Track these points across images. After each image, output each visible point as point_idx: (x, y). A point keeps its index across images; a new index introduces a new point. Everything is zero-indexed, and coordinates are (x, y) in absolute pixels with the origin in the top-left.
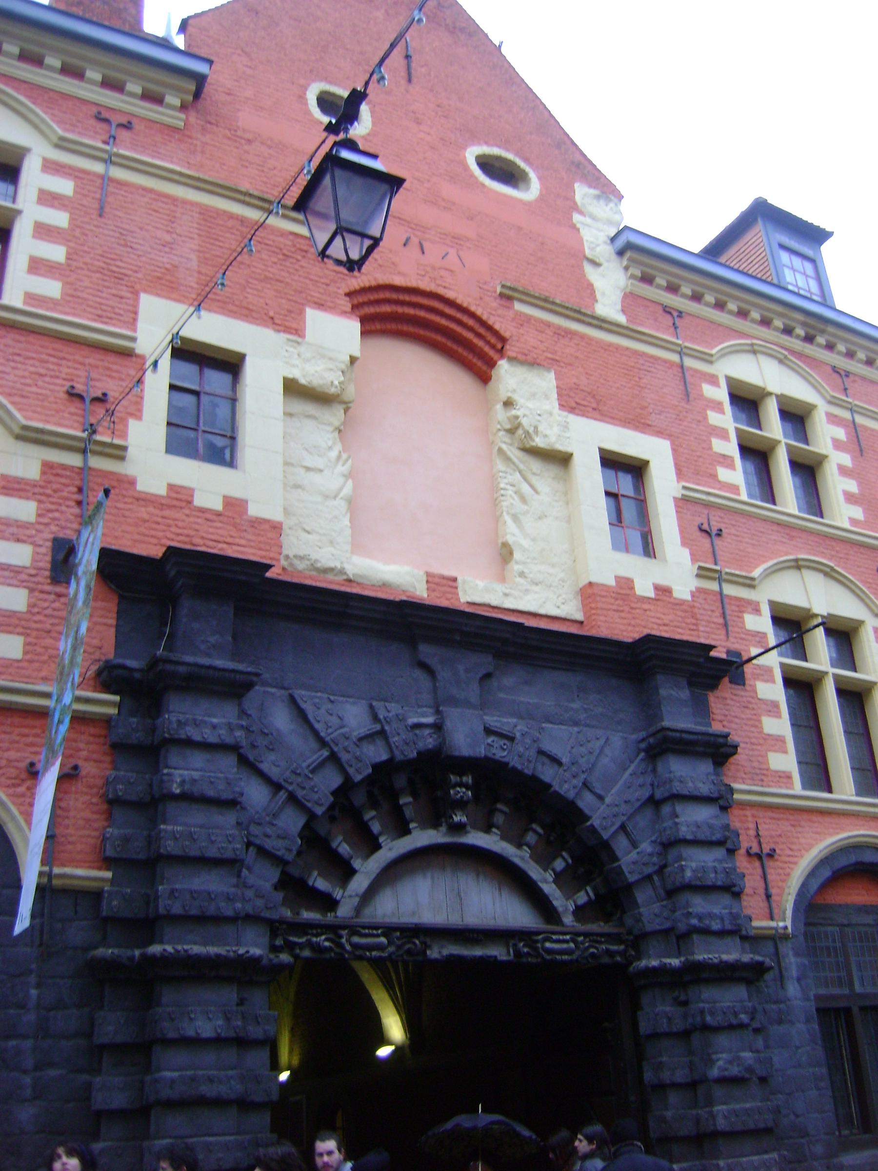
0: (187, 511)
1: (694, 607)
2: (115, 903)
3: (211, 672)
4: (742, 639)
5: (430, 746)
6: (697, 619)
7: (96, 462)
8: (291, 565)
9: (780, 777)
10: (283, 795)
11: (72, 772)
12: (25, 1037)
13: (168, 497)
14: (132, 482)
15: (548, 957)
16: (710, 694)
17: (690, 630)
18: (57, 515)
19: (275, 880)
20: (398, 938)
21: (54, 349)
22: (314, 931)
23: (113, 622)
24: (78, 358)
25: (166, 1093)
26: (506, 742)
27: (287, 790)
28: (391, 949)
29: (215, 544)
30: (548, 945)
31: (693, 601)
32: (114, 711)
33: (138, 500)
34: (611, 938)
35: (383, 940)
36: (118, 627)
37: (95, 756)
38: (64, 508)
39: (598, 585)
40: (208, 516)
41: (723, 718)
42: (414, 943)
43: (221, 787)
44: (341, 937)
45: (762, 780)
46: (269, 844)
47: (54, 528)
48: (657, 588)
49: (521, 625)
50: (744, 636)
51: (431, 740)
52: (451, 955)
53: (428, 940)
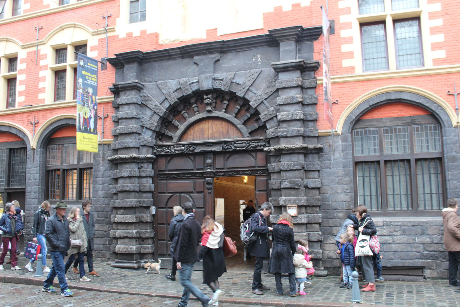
0: (131, 39)
1: (311, 7)
2: (113, 146)
4: (336, 13)
5: (196, 89)
6: (312, 12)
7: (110, 34)
8: (164, 43)
9: (348, 69)
10: (153, 112)
11: (107, 116)
12: (100, 177)
13: (127, 37)
14: (118, 36)
15: (235, 149)
16: (315, 42)
17: (308, 18)
18: (102, 52)
20: (187, 147)
21: (100, 7)
23: (115, 76)
24: (105, 7)
25: (119, 190)
26: (221, 82)
28: (185, 150)
29: (138, 46)
30: (235, 145)
31: (311, 5)
32: (113, 99)
33: (119, 41)
34: (259, 140)
35: (183, 148)
36: (116, 77)
37: (112, 111)
38: (103, 50)
39: (266, 13)
40: (137, 38)
41: (320, 51)
44: (171, 148)
45: (337, 72)
46: (148, 126)
47: (101, 56)
48: (293, 6)
49: (223, 41)
50: (336, 12)
53: (195, 147)
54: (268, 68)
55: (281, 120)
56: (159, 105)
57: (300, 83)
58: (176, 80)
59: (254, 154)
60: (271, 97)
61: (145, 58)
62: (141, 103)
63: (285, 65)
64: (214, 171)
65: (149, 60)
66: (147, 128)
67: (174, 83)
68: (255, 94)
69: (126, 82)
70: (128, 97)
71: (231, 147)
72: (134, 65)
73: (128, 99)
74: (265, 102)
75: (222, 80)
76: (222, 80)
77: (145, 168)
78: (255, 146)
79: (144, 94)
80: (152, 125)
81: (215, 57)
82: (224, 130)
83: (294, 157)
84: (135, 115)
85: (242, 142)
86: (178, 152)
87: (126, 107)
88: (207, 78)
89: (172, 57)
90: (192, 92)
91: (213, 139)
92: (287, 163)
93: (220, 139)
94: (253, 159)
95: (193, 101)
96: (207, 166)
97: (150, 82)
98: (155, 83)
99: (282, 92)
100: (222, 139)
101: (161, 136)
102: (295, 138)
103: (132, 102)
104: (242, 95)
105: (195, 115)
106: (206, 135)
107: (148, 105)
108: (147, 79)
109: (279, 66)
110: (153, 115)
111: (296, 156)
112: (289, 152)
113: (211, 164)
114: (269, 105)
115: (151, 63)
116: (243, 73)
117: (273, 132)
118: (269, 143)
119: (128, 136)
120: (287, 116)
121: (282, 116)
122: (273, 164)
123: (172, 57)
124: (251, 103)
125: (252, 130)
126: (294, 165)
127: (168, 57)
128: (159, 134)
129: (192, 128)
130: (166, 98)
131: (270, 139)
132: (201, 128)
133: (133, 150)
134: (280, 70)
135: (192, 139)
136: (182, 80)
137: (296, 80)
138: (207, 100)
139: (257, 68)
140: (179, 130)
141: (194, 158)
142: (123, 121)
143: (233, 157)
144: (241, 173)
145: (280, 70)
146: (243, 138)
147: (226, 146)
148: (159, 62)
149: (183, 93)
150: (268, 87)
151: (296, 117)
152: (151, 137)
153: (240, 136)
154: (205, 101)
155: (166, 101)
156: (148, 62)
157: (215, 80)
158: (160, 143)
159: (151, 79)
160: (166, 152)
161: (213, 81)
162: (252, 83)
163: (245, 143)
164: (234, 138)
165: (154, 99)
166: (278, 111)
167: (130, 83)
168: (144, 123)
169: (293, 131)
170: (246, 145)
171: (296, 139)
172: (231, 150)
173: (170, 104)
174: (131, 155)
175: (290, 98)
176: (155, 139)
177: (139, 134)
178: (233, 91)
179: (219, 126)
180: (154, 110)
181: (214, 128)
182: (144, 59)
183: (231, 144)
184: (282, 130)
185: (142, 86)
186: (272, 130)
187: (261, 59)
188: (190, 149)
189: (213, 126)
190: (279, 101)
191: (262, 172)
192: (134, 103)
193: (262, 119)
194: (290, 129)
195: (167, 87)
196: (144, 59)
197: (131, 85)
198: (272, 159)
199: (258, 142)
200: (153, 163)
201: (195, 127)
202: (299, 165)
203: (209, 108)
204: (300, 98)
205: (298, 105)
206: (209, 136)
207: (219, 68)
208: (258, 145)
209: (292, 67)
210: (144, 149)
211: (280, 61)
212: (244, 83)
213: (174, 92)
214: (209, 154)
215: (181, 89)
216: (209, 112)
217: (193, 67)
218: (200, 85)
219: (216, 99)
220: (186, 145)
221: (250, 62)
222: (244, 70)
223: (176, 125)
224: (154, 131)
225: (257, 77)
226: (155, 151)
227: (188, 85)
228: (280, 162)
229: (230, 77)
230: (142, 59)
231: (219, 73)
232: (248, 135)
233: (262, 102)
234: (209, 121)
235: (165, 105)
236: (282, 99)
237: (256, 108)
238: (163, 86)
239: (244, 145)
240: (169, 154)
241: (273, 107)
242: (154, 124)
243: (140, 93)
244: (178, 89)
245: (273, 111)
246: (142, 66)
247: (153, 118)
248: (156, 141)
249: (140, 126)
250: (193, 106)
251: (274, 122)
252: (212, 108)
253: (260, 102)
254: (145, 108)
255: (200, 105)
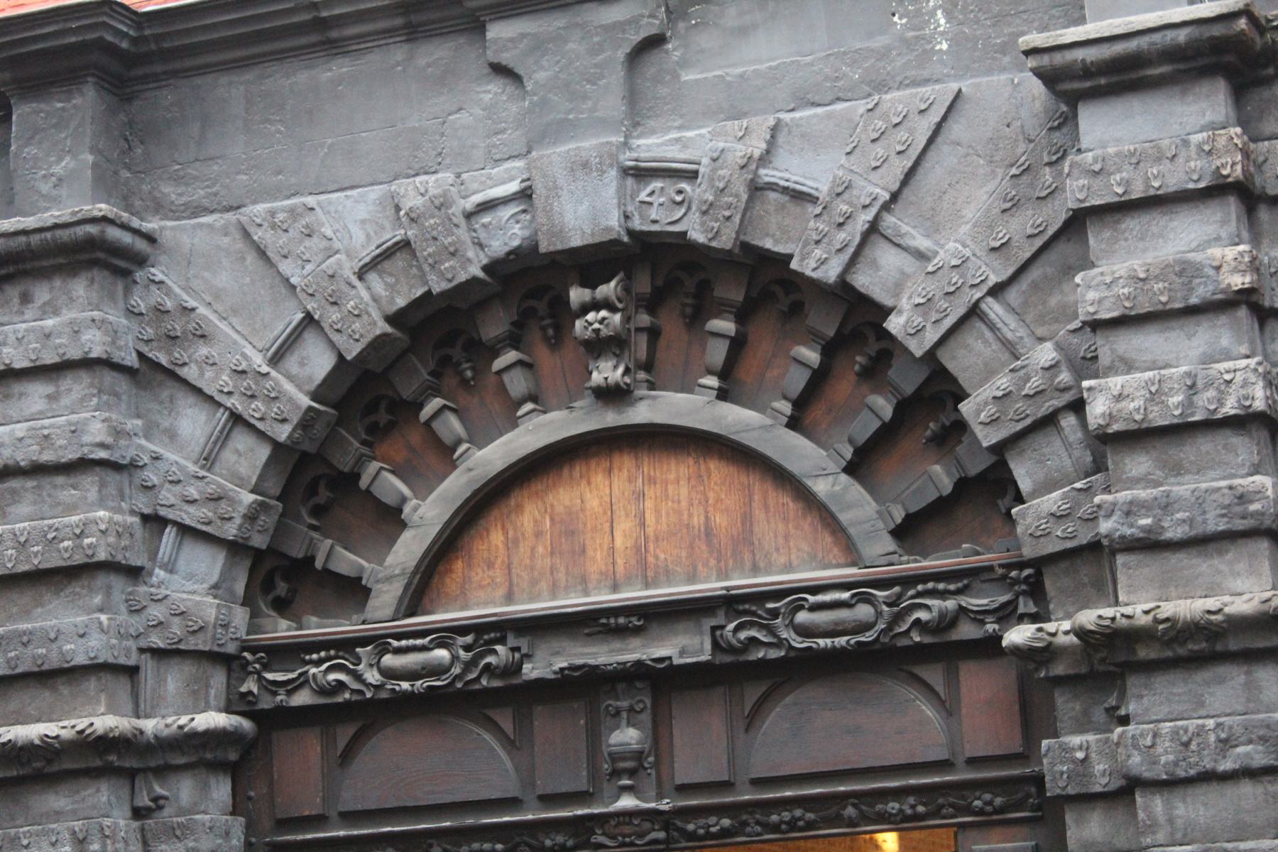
3: (59, 233)
5: (516, 243)
10: (222, 416)
15: (799, 643)
19: (215, 578)
20: (467, 648)
22: (315, 656)
26: (684, 185)
27: (227, 408)
28: (456, 670)
30: (802, 617)
34: (967, 578)
35: (442, 654)
42: (495, 652)
43: (62, 442)
44: (358, 661)
46: (191, 515)
51: (516, 229)
52: (573, 668)
53: (524, 643)
54: (1003, 77)
55: (1115, 427)
56: (265, 369)
57: (1233, 168)
58: (375, 193)
59: (934, 675)
60: (1035, 273)
61: (153, 47)
62: (141, 355)
63: (1119, 48)
64: (665, 805)
65: (178, 65)
66: (186, 531)
67: (363, 212)
68: (921, 256)
69: (30, 222)
70: (49, 323)
71: (771, 630)
72: (77, 101)
73: (48, 336)
74: (993, 308)
75: (692, 176)
76: (692, 176)
77: (182, 813)
78: (942, 615)
79: (156, 296)
80: (223, 507)
81: (634, 21)
82: (719, 520)
83: (1221, 681)
84: (102, 446)
85: (845, 595)
86: (405, 685)
87: (36, 395)
88: (585, 165)
89: (334, 34)
90: (485, 269)
91: (647, 586)
92: (1175, 733)
93: (692, 578)
94: (929, 711)
95: (494, 326)
96: (616, 774)
97: (198, 210)
98: (230, 216)
99: (1107, 234)
100: (707, 580)
101: (286, 578)
102: (1220, 553)
103: (74, 354)
104: (831, 273)
105: (514, 423)
106: (597, 560)
107: (190, 373)
108: (169, 191)
109: (1079, 54)
110: (224, 438)
111: (1235, 676)
112: (1181, 651)
113: (639, 755)
114: (1022, 332)
115: (198, 81)
116: (829, 116)
117: (1058, 517)
118: (1036, 590)
119: (57, 593)
120: (1156, 396)
121: (1119, 397)
122: (1076, 740)
123: (334, 34)
124: (894, 324)
125: (914, 508)
126: (1226, 744)
127: (313, 38)
128: (268, 565)
129: (495, 513)
130: (309, 320)
131: (1040, 563)
132: (560, 509)
133: (92, 684)
134: (1088, 84)
135: (501, 592)
136: (413, 193)
137: (1199, 147)
138: (591, 316)
139: (926, 82)
140: (407, 535)
141: (523, 721)
142: (14, 492)
143: (788, 700)
144: (850, 811)
145: (1088, 84)
146: (854, 564)
147: (737, 629)
148: (249, 76)
149: (423, 278)
150: (1012, 206)
151: (1221, 403)
152: (215, 586)
153: (836, 554)
154: (579, 324)
155: (310, 337)
156: (175, 74)
157: (641, 174)
158: (282, 630)
159: (198, 194)
160: (322, 691)
161: (630, 181)
162: (895, 186)
163: (868, 599)
164: (789, 568)
165: (223, 326)
166: (1087, 365)
167: (56, 226)
168: (168, 495)
169: (1199, 501)
170: (879, 614)
171: (1230, 556)
172: (774, 654)
173: (341, 357)
174: (82, 724)
175: (1164, 272)
176: (247, 601)
177: (134, 573)
178: (768, 244)
179: (684, 491)
180: (229, 402)
181: (649, 504)
182: (146, 58)
183: (775, 614)
184: (1124, 496)
185: (141, 245)
186: (1052, 501)
187: (949, 15)
188: (490, 659)
189: (640, 496)
190: (1092, 295)
191: (998, 801)
192: (87, 364)
193: (979, 431)
194: (1182, 488)
195: (315, 243)
196: (146, 58)
197: (64, 235)
198: (1066, 705)
199: (958, 592)
200: (235, 771)
201: (519, 508)
202: (1264, 740)
203: (607, 372)
204: (1235, 270)
205: (1223, 319)
206: (620, 561)
207: (663, 91)
208: (962, 610)
209: (1172, 54)
210: (174, 680)
211: (1081, 20)
212: (842, 190)
213: (361, 275)
214: (621, 687)
215: (413, 254)
216: (612, 395)
217: (487, 97)
218: (542, 219)
219: (652, 304)
220: (462, 630)
221: (880, 42)
222: (838, 99)
223: (389, 500)
224: (235, 548)
225: (931, 141)
226: (251, 685)
227: (462, 221)
228: (1125, 721)
229: (739, 151)
230: (130, 60)
231: (669, 129)
232: (889, 544)
233: (974, 312)
234: (617, 459)
235: (302, 364)
236: (1109, 286)
237: (931, 354)
238: (283, 239)
239: (864, 612)
240: (347, 703)
241: (1048, 345)
242: (232, 501)
243: (127, 292)
244: (387, 254)
245: (1052, 368)
246: (137, 103)
247: (228, 456)
248: (255, 614)
249: (136, 520)
250: (499, 363)
251: (1068, 446)
252: (627, 371)
253: (961, 311)
254: (165, 394)
255: (543, 355)
